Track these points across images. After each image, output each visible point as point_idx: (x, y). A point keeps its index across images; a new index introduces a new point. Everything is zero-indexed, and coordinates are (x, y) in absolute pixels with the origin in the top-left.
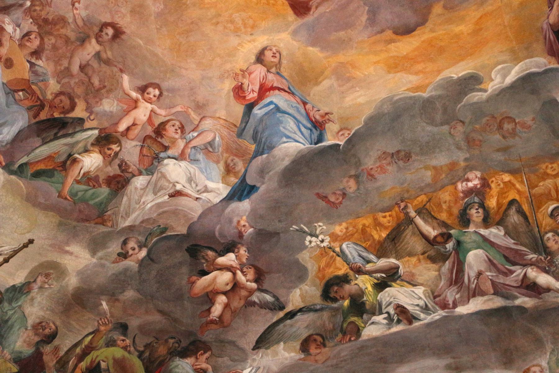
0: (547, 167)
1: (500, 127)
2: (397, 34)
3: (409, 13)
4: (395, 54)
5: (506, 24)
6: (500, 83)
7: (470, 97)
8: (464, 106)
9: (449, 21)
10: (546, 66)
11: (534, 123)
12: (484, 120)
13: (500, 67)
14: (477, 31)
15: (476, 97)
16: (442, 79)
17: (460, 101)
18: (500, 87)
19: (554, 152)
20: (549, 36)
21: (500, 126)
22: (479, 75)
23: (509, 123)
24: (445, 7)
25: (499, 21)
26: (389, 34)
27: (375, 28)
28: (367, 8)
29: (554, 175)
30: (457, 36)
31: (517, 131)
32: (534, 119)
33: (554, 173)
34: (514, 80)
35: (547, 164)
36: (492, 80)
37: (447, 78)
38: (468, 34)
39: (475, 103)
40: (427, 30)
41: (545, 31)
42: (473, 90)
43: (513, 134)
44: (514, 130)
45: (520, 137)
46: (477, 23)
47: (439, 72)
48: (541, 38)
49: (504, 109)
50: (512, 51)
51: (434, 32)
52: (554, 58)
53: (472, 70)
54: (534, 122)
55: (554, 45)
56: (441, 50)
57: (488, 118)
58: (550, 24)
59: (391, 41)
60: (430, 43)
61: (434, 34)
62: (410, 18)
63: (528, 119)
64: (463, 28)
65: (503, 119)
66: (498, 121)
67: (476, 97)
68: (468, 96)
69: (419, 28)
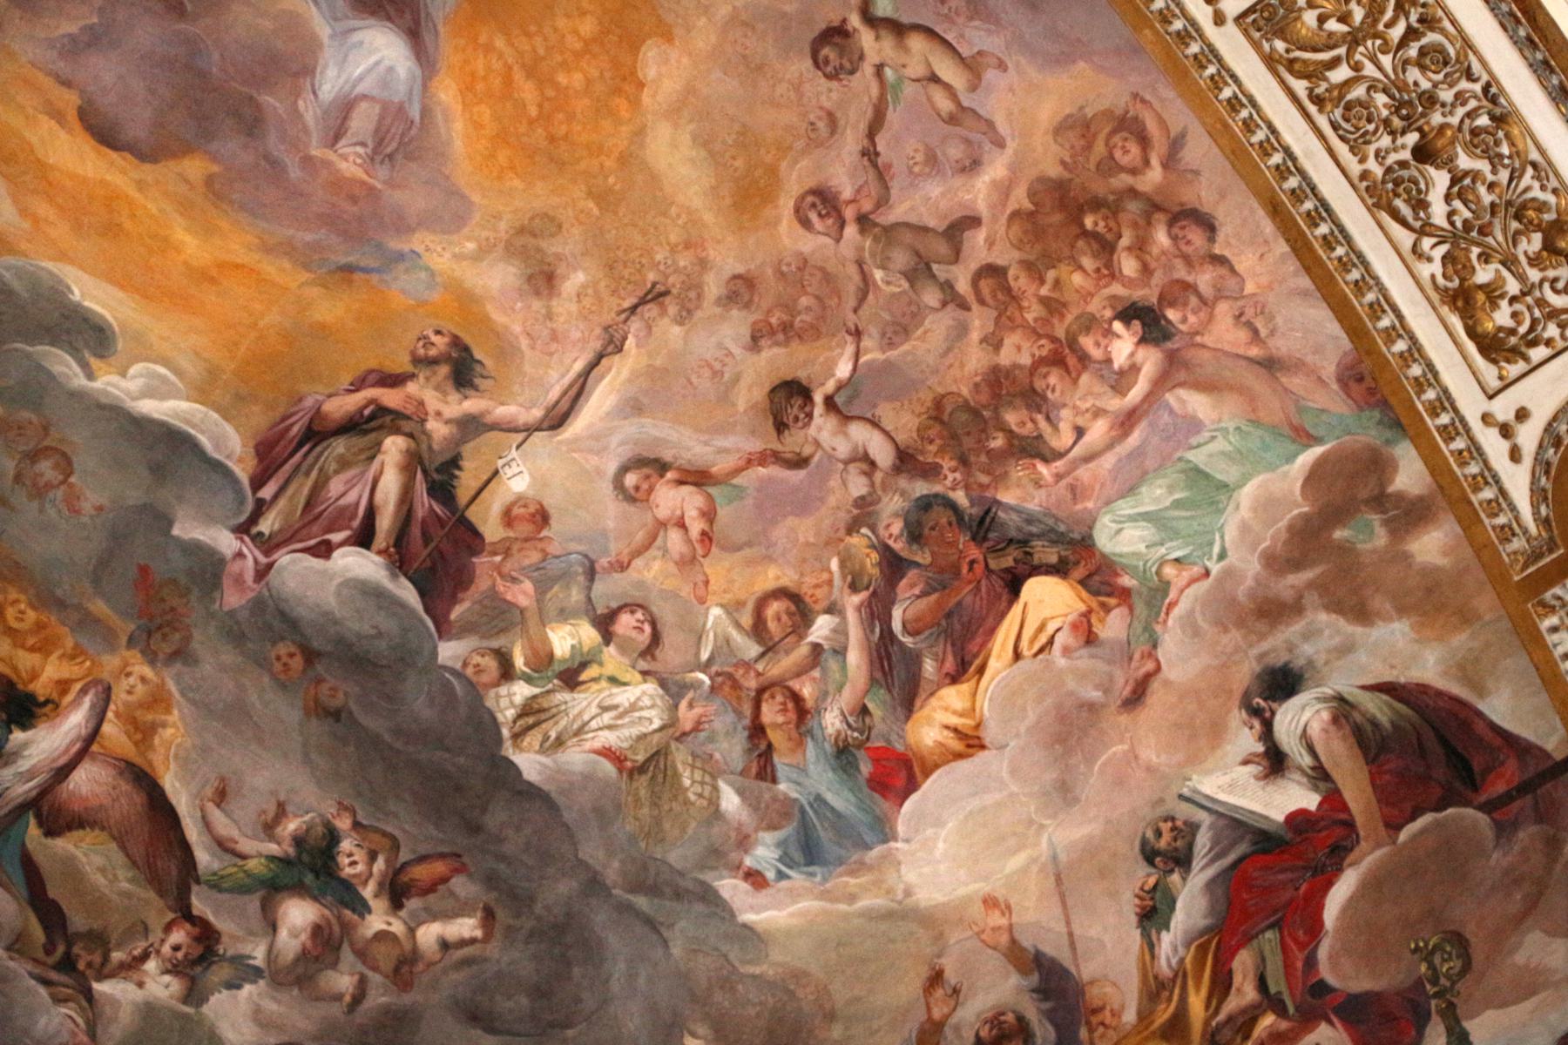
0: (16, 601)
1: (34, 456)
2: (81, 119)
3: (147, 114)
4: (34, 140)
5: (261, 324)
6: (128, 393)
7: (57, 355)
8: (28, 356)
9: (185, 207)
10: (228, 457)
11: (92, 517)
12: (26, 415)
13: (162, 370)
14: (204, 277)
15: (64, 365)
16: (50, 273)
17: (32, 339)
18: (117, 397)
19: (59, 592)
20: (292, 425)
21: (35, 455)
22: (114, 340)
23: (56, 466)
24: (209, 181)
25: (258, 307)
26: (70, 100)
27: (62, 64)
28: (95, 20)
29: (10, 628)
30: (166, 245)
31: (51, 495)
32: (100, 509)
33: (15, 625)
34: (156, 416)
35: (22, 597)
36: (123, 374)
37: (61, 281)
38: (185, 263)
39: (51, 376)
40: (135, 175)
41: (301, 406)
42: (75, 352)
43: (40, 492)
44: (49, 486)
45: (41, 511)
46: (222, 266)
47: (63, 257)
48: (281, 411)
49: (78, 437)
50: (213, 373)
51: (140, 190)
52: (255, 462)
53: (115, 318)
54: (94, 513)
55: (282, 443)
56: (111, 230)
57: (34, 418)
58: (319, 408)
59: (58, 116)
60: (112, 199)
61: (132, 192)
62: (137, 123)
63: (92, 498)
64: (191, 245)
65: (56, 450)
66: (46, 443)
67: (64, 365)
68: (53, 350)
69: (129, 156)
